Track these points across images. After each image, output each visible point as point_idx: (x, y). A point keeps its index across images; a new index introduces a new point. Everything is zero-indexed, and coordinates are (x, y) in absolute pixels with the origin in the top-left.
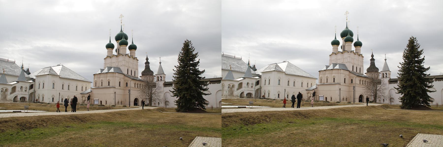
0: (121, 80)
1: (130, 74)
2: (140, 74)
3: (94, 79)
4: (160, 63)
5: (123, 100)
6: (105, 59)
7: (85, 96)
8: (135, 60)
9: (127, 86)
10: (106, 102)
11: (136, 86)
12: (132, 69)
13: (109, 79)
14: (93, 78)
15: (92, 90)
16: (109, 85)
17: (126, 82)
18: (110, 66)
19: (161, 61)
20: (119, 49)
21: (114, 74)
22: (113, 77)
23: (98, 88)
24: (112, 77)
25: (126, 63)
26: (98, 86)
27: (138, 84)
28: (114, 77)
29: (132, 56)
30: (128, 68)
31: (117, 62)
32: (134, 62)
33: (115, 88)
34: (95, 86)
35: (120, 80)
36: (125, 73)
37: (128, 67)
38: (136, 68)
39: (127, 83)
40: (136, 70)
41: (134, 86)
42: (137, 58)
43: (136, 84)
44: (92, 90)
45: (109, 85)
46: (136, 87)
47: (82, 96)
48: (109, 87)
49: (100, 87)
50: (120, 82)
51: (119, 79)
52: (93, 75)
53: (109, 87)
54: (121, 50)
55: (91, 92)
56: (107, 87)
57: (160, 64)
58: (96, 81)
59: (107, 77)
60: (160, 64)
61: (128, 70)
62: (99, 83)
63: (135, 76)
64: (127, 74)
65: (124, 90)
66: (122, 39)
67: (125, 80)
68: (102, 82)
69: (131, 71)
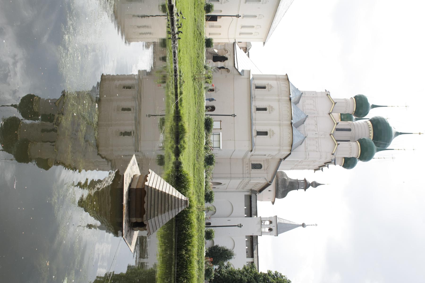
4: (303, 225)
9: (252, 168)
13: (273, 133)
17: (262, 163)
19: (307, 227)
20: (350, 130)
22: (280, 145)
23: (251, 97)
24: (279, 121)
45: (259, 133)
52: (286, 75)
53: (254, 133)
55: (238, 73)
56: (254, 128)
57: (300, 225)
58: (271, 87)
59: (280, 125)
60: (300, 225)
67: (267, 160)
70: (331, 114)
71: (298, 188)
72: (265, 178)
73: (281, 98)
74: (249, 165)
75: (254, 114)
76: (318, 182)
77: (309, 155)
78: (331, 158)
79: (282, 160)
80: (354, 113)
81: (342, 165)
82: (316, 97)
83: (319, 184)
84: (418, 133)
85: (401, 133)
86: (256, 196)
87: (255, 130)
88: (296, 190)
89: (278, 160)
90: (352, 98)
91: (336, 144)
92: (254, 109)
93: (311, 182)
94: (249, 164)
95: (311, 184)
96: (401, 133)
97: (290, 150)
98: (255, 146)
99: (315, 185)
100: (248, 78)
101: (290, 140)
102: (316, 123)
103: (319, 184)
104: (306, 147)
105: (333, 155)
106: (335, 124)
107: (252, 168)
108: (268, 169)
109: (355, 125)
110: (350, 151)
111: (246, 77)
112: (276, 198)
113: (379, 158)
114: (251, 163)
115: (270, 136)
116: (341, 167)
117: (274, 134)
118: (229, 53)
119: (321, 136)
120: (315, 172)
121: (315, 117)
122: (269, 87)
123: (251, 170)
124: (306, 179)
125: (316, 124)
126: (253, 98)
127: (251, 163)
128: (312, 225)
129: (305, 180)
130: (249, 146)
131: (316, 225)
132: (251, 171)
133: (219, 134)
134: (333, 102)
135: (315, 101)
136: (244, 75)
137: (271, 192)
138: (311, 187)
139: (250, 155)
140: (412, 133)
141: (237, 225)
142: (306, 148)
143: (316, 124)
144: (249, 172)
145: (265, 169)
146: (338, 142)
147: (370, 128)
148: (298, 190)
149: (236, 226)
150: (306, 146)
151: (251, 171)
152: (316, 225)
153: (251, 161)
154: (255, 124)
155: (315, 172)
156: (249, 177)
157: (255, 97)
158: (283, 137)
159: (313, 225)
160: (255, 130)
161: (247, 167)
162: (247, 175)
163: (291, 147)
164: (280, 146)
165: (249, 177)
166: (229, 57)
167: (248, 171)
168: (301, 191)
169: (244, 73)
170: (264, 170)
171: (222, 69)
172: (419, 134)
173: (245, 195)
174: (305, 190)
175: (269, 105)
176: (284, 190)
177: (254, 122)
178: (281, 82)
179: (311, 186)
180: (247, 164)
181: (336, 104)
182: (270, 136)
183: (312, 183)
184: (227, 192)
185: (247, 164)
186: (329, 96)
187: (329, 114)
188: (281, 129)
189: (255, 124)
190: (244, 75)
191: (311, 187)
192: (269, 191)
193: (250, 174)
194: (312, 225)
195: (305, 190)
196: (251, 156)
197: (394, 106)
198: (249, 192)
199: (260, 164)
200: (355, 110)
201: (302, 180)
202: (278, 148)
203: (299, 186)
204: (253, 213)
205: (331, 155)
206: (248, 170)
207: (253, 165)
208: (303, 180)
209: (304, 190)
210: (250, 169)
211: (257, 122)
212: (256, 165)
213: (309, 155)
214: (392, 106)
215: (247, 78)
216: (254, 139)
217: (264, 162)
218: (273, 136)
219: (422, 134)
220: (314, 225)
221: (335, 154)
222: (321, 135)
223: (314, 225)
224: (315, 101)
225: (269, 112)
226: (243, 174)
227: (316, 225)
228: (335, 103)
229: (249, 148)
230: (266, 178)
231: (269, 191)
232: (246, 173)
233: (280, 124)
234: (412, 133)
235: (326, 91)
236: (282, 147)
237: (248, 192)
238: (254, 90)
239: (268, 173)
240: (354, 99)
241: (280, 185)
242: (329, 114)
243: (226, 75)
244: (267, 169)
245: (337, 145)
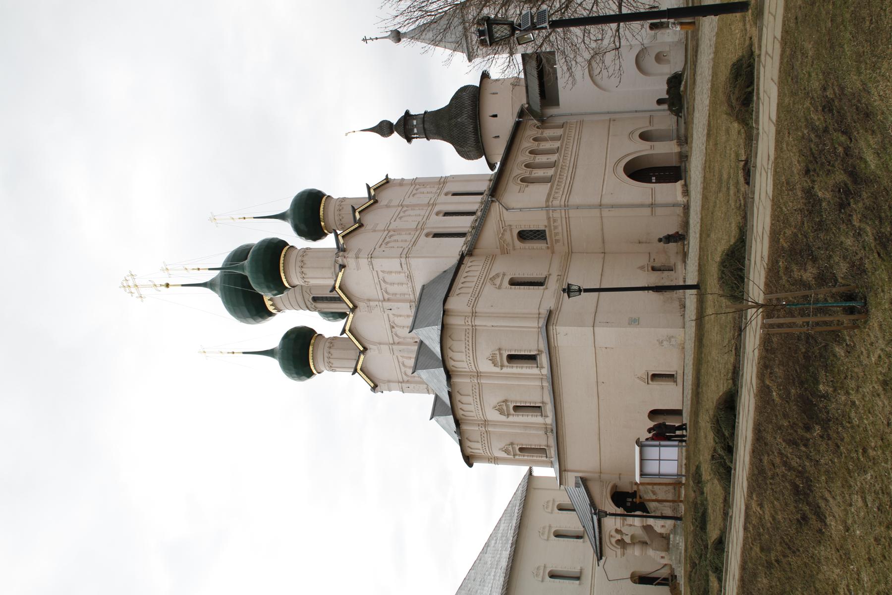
0: (497, 275)
1: (464, 224)
2: (479, 167)
3: (495, 460)
5: (643, 261)
6: (374, 388)
7: (617, 531)
8: (385, 197)
9: (545, 231)
10: (655, 377)
11: (539, 173)
12: (437, 214)
14: (492, 465)
15: (571, 478)
16: (532, 358)
17: (518, 243)
18: (414, 355)
21: (452, 321)
25: (390, 245)
26: (542, 432)
27: (528, 166)
28: (478, 322)
29: (354, 210)
30: (425, 231)
31: (387, 305)
32: (395, 202)
33: (550, 313)
34: (544, 459)
35: (498, 281)
36: (458, 245)
37: (418, 237)
38: (434, 190)
39: (524, 236)
40: (445, 190)
41: (544, 188)
42: (369, 188)
43: (526, 173)
44: (571, 478)
45: (532, 358)
46: (550, 172)
47: (619, 551)
48: (544, 359)
49: (550, 420)
50: (514, 283)
51: (488, 289)
52: (470, 465)
54: (313, 282)
56: (545, 371)
58: (506, 451)
61: (436, 235)
62: (526, 426)
63: (481, 194)
64: (464, 239)
65: (570, 253)
66: (247, 273)
67: (504, 251)
68: (516, 408)
69: (447, 214)
70: (362, 349)
71: (426, 119)
72: (507, 210)
73: (482, 427)
74: (554, 238)
75: (548, 398)
76: (376, 136)
77: (401, 264)
78: (345, 257)
79: (467, 254)
80: (312, 341)
81: (324, 200)
82: (401, 383)
83: (372, 130)
84: (170, 287)
85: (204, 285)
86: (528, 103)
87: (542, 367)
88: (429, 110)
89: (477, 251)
90: (319, 373)
91: (340, 288)
92: (549, 409)
93: (393, 135)
94: (554, 241)
95: (394, 130)
96: (204, 285)
97: (446, 313)
98: (540, 325)
99: (384, 129)
100: (565, 471)
101: (449, 343)
102: (393, 330)
103: (372, 130)
104: (409, 279)
105: (342, 264)
106: (350, 331)
107: (545, 231)
108: (502, 231)
109: (306, 308)
110: (303, 269)
111: (569, 473)
112: (478, 86)
113: (244, 218)
114: (547, 244)
115: (501, 355)
116: (327, 193)
117: (491, 358)
118: (613, 540)
119: (378, 305)
120: (387, 176)
121: (398, 343)
122: (510, 448)
123: (546, 226)
124: (406, 140)
125: (393, 327)
126: (549, 430)
127: (547, 244)
128: (377, 38)
129: (409, 140)
130: (555, 335)
131: (365, 40)
132: (546, 224)
133: (642, 474)
134: (361, 373)
135: (403, 375)
136: (576, 477)
137: (491, 115)
138: (394, 121)
139: (551, 277)
140: (183, 285)
141: (582, 293)
142: (410, 277)
143: (393, 327)
144: (552, 223)
145: (509, 232)
146: (334, 295)
147: (271, 305)
148: (426, 112)
149: (586, 290)
150: (410, 281)
151: (546, 224)
152: (366, 40)
153: (548, 248)
154: (542, 378)
155: (387, 176)
156: (551, 211)
157: (546, 434)
158: (467, 350)
159: (372, 40)
160: (542, 367)
161: (556, 234)
162: (557, 215)
163: (445, 323)
164: (472, 326)
165: (551, 211)
166: (613, 533)
167: (556, 224)
168: (417, 110)
169: (574, 482)
170: (511, 230)
171: (630, 492)
172: (170, 284)
173: (555, 102)
174: (407, 113)
175: (508, 417)
176: (459, 120)
177: (545, 384)
178: (481, 453)
179: (395, 124)
180: (557, 241)
181: (353, 370)
182: (501, 355)
183: (391, 133)
184: (608, 113)
185: (557, 241)
186: (372, 385)
187: (365, 349)
188: (473, 367)
189: (541, 377)
190: (576, 477)
191: (394, 121)
192: (495, 116)
193: (549, 218)
194: (377, 38)
195: (407, 113)
196: (550, 275)
197: (228, 353)
198: (548, 118)
199: (525, 239)
200: (311, 349)
201: (417, 138)
202: (478, 322)
203: (422, 126)
204: (534, 63)
205: (346, 264)
206: (556, 227)
207: (543, 236)
208: (414, 138)
209: (412, 113)
210: (550, 231)
211: (538, 383)
212: (535, 237)
213: (401, 264)
214: (233, 353)
215: (568, 471)
216: (543, 346)
217: (514, 246)
218: (494, 356)
219: (163, 285)
220: (371, 39)
221: (337, 266)
222: (377, 305)
223: (371, 39)
224: (403, 375)
225: (510, 403)
226: (567, 216)
227: (365, 40)
228: (355, 371)
229: (555, 331)
230: (503, 209)
231: (495, 116)
232: (559, 221)
233: (478, 376)
234: (183, 285)
235: (382, 392)
236: (467, 323)
237: (552, 116)
238: (547, 446)
239: (500, 222)
240: (314, 371)
241: (470, 130)
242: (365, 349)
243: (620, 479)
244: (504, 231)
245: (337, 285)
